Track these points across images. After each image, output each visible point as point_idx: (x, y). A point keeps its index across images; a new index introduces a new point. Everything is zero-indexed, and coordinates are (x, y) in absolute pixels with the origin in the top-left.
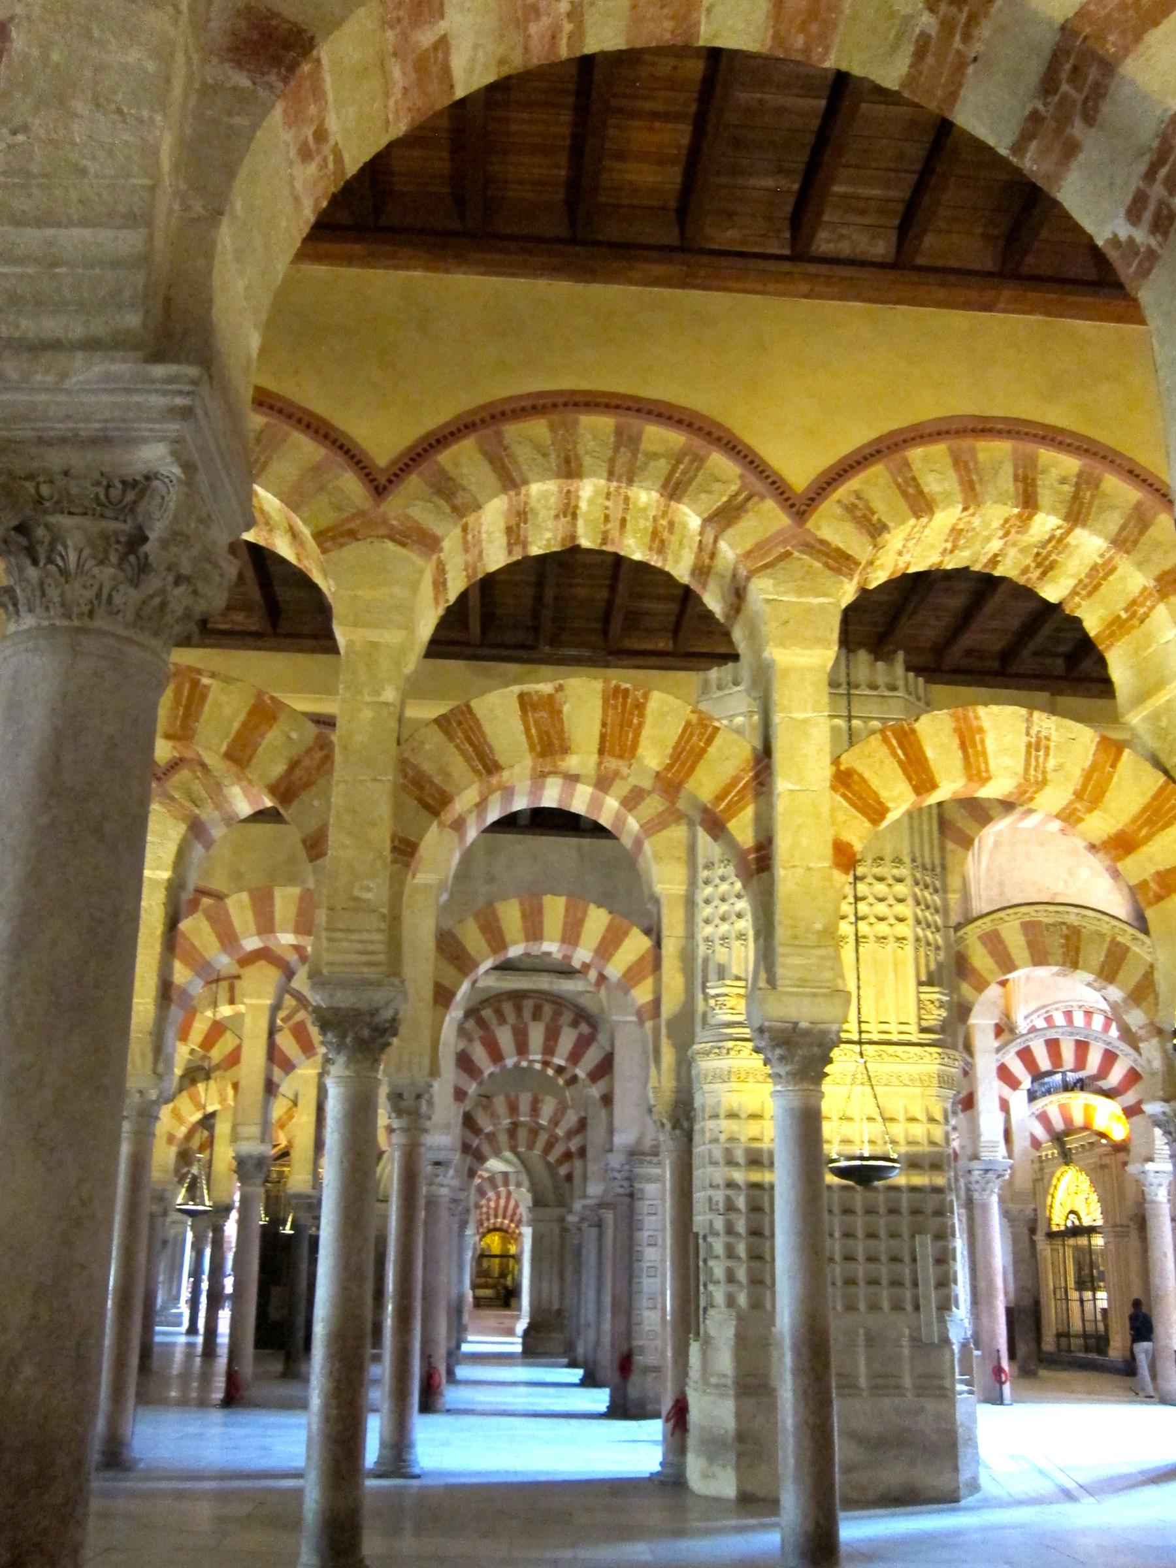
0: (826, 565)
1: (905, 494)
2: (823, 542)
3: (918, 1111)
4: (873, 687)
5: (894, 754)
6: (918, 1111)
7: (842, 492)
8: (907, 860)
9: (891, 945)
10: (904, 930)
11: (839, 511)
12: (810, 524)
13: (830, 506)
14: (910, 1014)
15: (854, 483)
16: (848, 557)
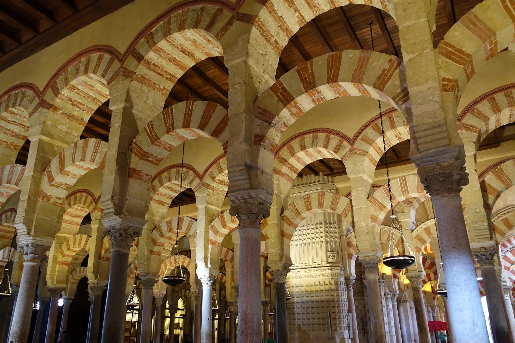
0: (206, 188)
1: (218, 169)
2: (206, 183)
3: (327, 282)
4: (315, 182)
5: (220, 221)
6: (327, 282)
7: (209, 172)
8: (323, 222)
9: (320, 243)
10: (322, 239)
11: (208, 176)
12: (203, 180)
13: (207, 175)
14: (324, 259)
15: (211, 170)
16: (208, 185)
